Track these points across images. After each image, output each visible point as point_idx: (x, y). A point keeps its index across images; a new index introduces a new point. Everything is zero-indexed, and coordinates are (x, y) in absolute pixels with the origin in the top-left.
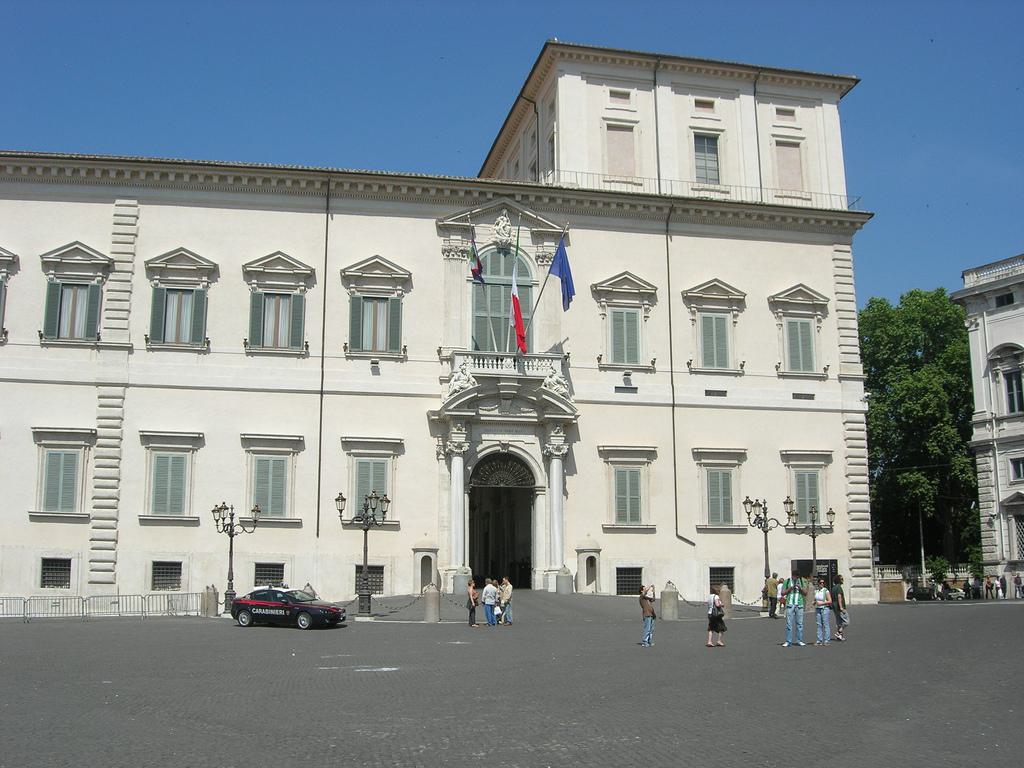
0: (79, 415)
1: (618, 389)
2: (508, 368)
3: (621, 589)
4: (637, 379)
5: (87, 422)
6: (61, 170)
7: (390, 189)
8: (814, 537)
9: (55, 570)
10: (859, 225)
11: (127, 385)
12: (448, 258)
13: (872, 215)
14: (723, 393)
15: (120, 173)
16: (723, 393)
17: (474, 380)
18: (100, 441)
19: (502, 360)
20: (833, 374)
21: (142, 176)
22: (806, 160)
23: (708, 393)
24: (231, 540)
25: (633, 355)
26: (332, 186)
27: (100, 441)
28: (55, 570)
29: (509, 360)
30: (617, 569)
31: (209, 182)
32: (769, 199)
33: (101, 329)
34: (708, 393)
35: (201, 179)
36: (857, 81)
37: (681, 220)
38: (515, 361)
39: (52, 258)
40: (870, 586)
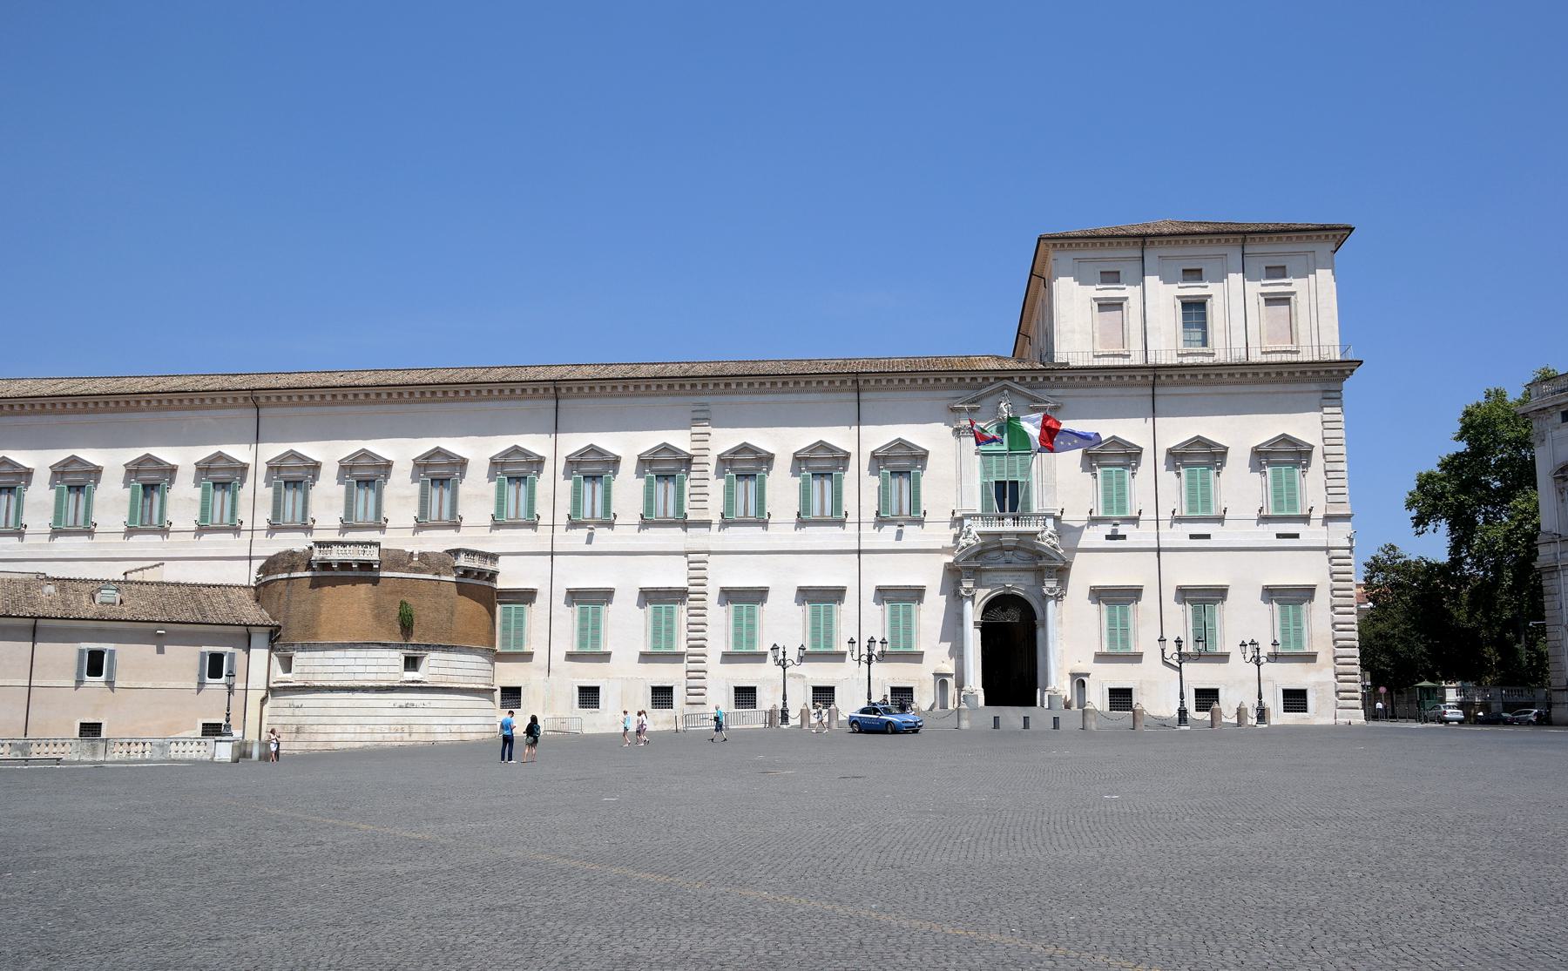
0: (672, 575)
1: (1108, 537)
2: (1008, 526)
3: (1114, 705)
4: (1122, 529)
5: (680, 582)
6: (648, 387)
7: (908, 382)
8: (1259, 666)
9: (662, 696)
10: (1349, 372)
11: (709, 553)
12: (959, 437)
13: (1361, 362)
14: (1208, 536)
15: (693, 386)
16: (1208, 536)
17: (978, 537)
18: (691, 596)
19: (1003, 519)
20: (1318, 514)
21: (711, 387)
22: (1296, 314)
23: (1192, 537)
24: (784, 671)
25: (1122, 509)
26: (861, 383)
27: (691, 596)
28: (662, 696)
29: (1008, 520)
30: (1110, 690)
31: (763, 387)
32: (1256, 357)
33: (686, 510)
34: (1192, 537)
35: (757, 386)
36: (1352, 230)
37: (1163, 385)
38: (1014, 519)
39: (646, 457)
40: (1357, 708)
